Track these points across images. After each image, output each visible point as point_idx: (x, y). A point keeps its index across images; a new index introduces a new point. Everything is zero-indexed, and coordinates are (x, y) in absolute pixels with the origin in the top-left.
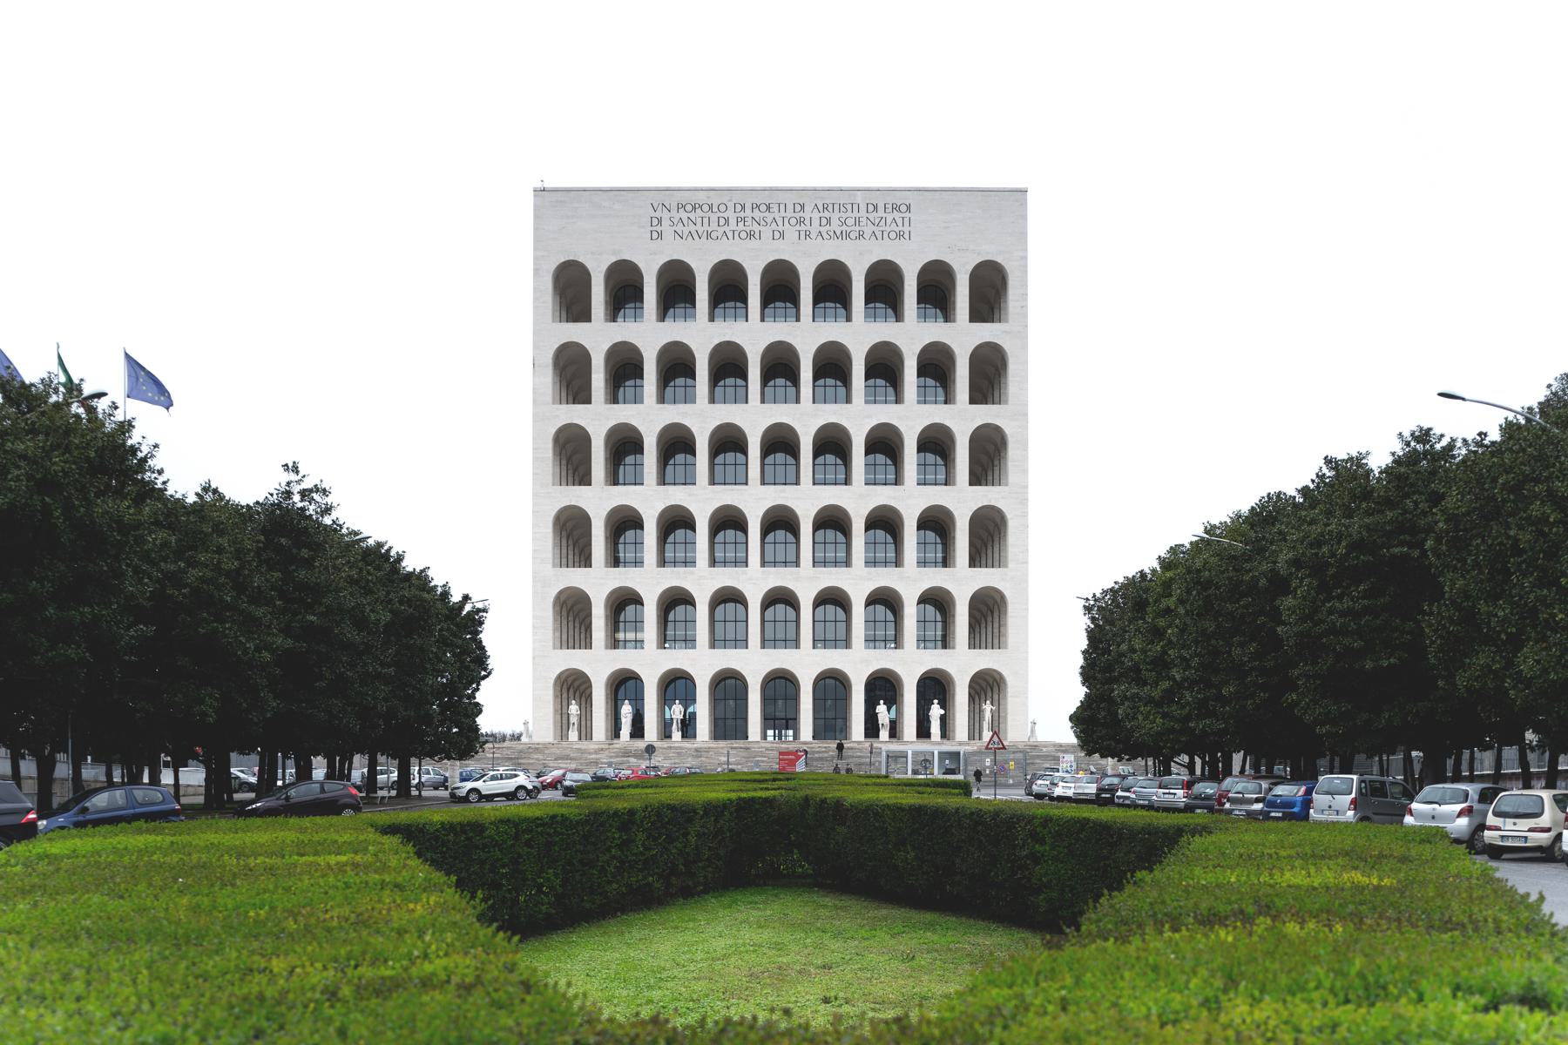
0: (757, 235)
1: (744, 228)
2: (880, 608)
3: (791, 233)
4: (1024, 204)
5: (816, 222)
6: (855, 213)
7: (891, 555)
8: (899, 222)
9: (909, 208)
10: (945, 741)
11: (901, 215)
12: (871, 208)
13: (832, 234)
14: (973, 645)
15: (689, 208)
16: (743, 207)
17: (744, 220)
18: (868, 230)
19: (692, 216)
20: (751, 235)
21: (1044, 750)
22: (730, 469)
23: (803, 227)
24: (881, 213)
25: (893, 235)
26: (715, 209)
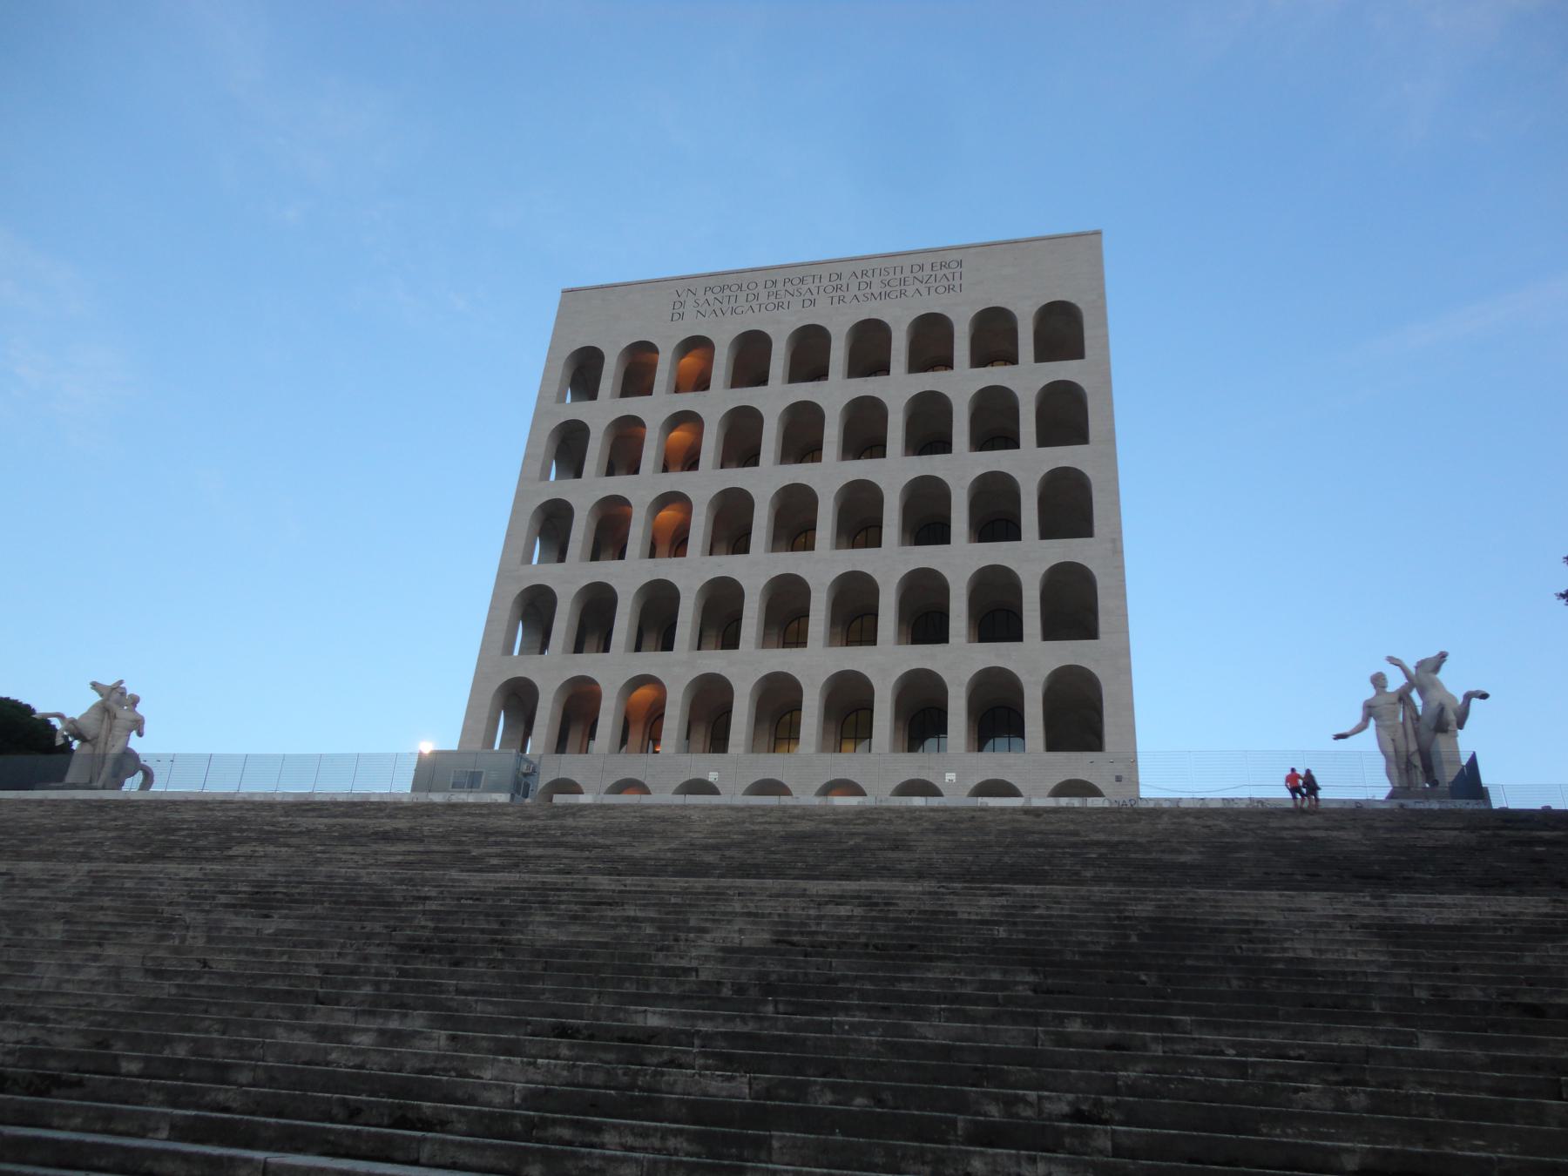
0: (785, 306)
3: (823, 301)
4: (1098, 248)
5: (854, 289)
6: (898, 275)
8: (950, 277)
9: (960, 264)
12: (916, 268)
20: (778, 306)
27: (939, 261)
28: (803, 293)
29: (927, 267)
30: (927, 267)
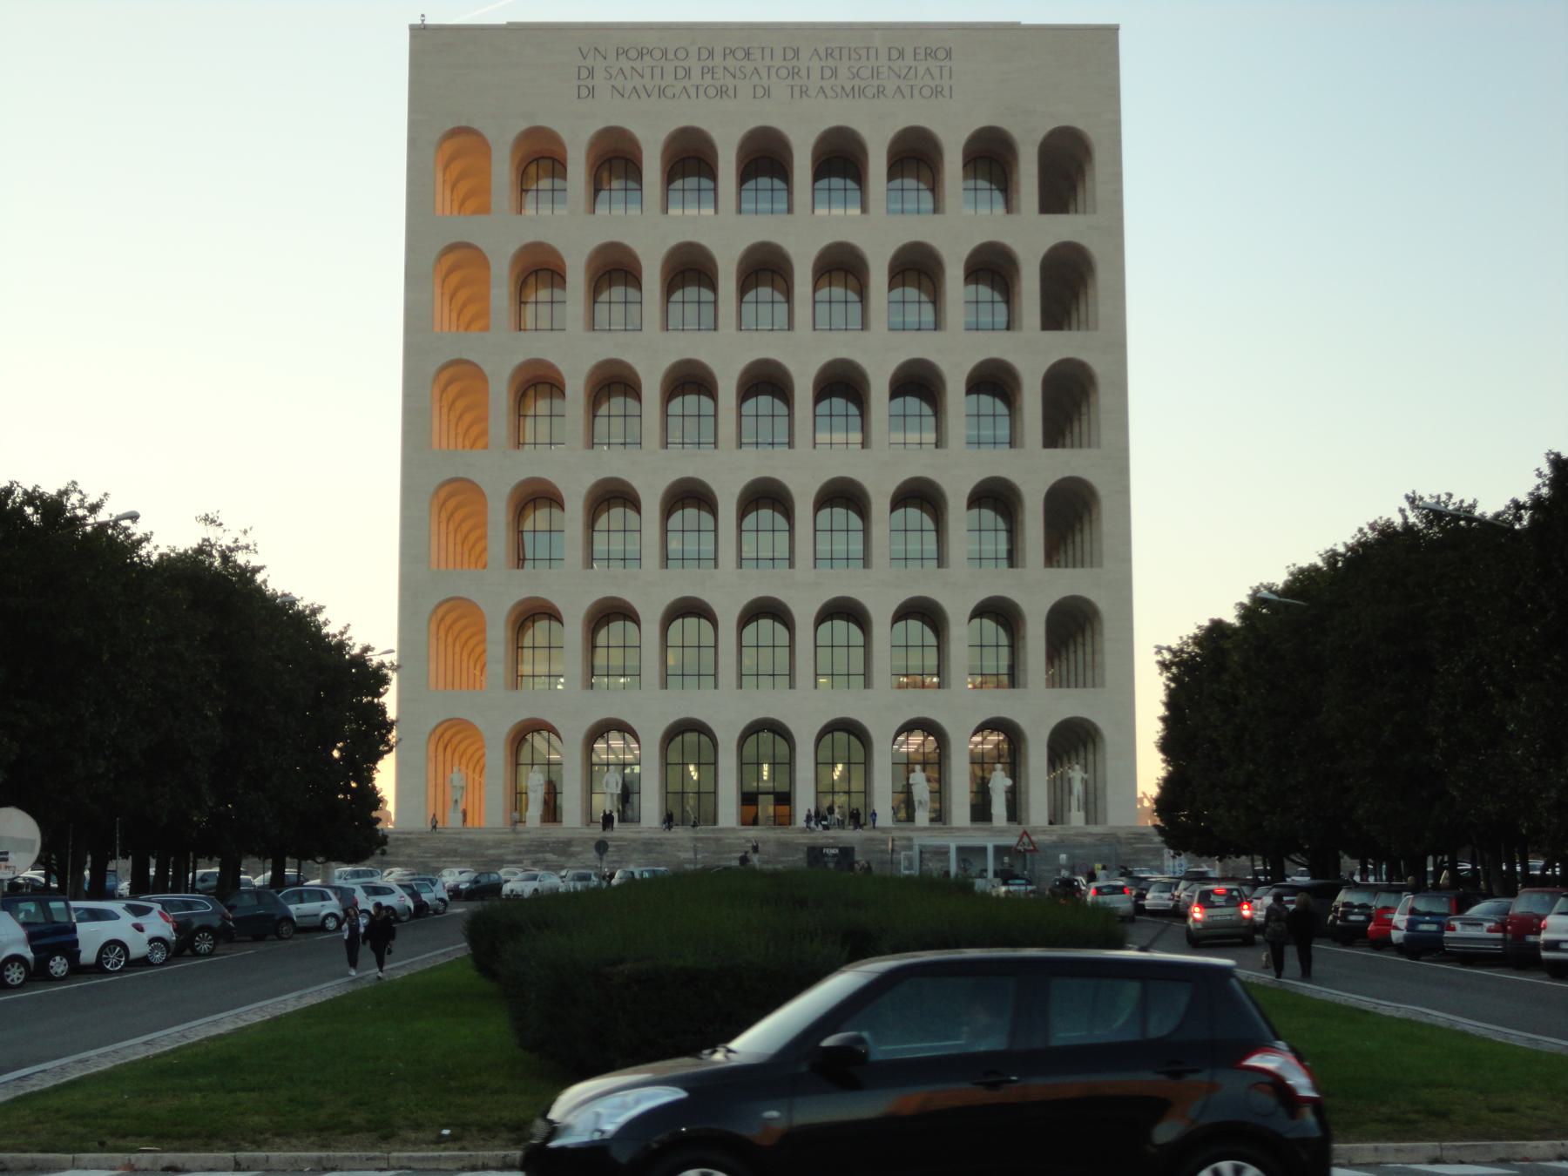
0: (731, 92)
2: (915, 626)
5: (816, 75)
8: (936, 72)
9: (949, 54)
11: (942, 64)
12: (895, 54)
14: (1052, 683)
15: (633, 54)
16: (711, 54)
17: (712, 71)
19: (638, 65)
20: (722, 92)
22: (691, 424)
24: (909, 61)
25: (926, 92)
26: (671, 56)
28: (748, 75)
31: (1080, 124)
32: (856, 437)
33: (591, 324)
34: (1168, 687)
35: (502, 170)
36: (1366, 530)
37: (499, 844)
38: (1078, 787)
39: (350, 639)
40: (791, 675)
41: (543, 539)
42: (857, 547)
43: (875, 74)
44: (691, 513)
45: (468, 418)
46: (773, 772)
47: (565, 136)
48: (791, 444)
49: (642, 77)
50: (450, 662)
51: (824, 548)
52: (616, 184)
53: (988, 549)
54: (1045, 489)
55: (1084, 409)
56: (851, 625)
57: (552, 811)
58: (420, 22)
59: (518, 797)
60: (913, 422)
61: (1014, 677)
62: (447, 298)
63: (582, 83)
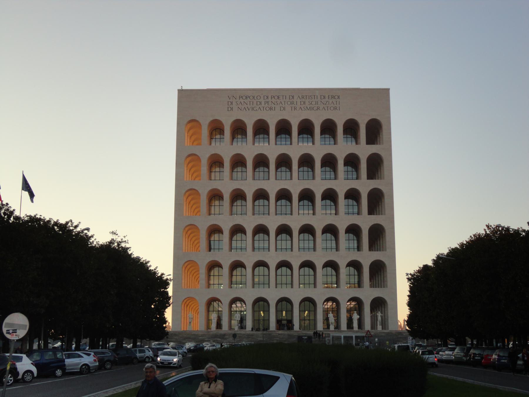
0: (273, 109)
1: (268, 106)
2: (329, 269)
5: (299, 103)
6: (316, 100)
7: (334, 245)
8: (335, 103)
9: (339, 97)
10: (360, 330)
13: (306, 108)
14: (372, 286)
15: (244, 98)
16: (267, 97)
18: (321, 106)
19: (245, 101)
20: (271, 109)
21: (404, 334)
22: (261, 208)
23: (293, 105)
24: (327, 99)
25: (332, 108)
26: (255, 98)
27: (331, 95)
29: (327, 96)
30: (327, 96)
31: (378, 118)
32: (311, 212)
33: (232, 178)
34: (410, 286)
35: (205, 131)
36: (473, 236)
37: (203, 335)
38: (379, 318)
39: (157, 271)
40: (292, 284)
41: (216, 243)
42: (312, 245)
43: (317, 103)
44: (261, 235)
45: (194, 207)
46: (286, 314)
47: (223, 122)
48: (291, 214)
49: (247, 104)
50: (189, 280)
51: (302, 245)
52: (239, 136)
53: (351, 245)
54: (369, 227)
55: (380, 203)
56: (310, 269)
57: (219, 325)
58: (181, 89)
59: (208, 321)
60: (328, 207)
61: (360, 284)
62: (188, 170)
63: (228, 106)
